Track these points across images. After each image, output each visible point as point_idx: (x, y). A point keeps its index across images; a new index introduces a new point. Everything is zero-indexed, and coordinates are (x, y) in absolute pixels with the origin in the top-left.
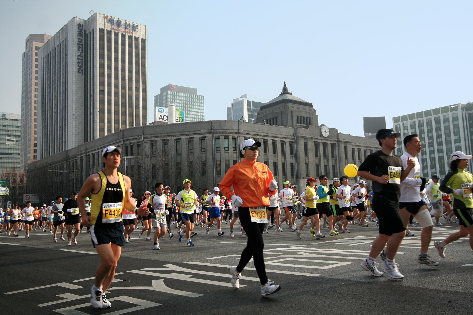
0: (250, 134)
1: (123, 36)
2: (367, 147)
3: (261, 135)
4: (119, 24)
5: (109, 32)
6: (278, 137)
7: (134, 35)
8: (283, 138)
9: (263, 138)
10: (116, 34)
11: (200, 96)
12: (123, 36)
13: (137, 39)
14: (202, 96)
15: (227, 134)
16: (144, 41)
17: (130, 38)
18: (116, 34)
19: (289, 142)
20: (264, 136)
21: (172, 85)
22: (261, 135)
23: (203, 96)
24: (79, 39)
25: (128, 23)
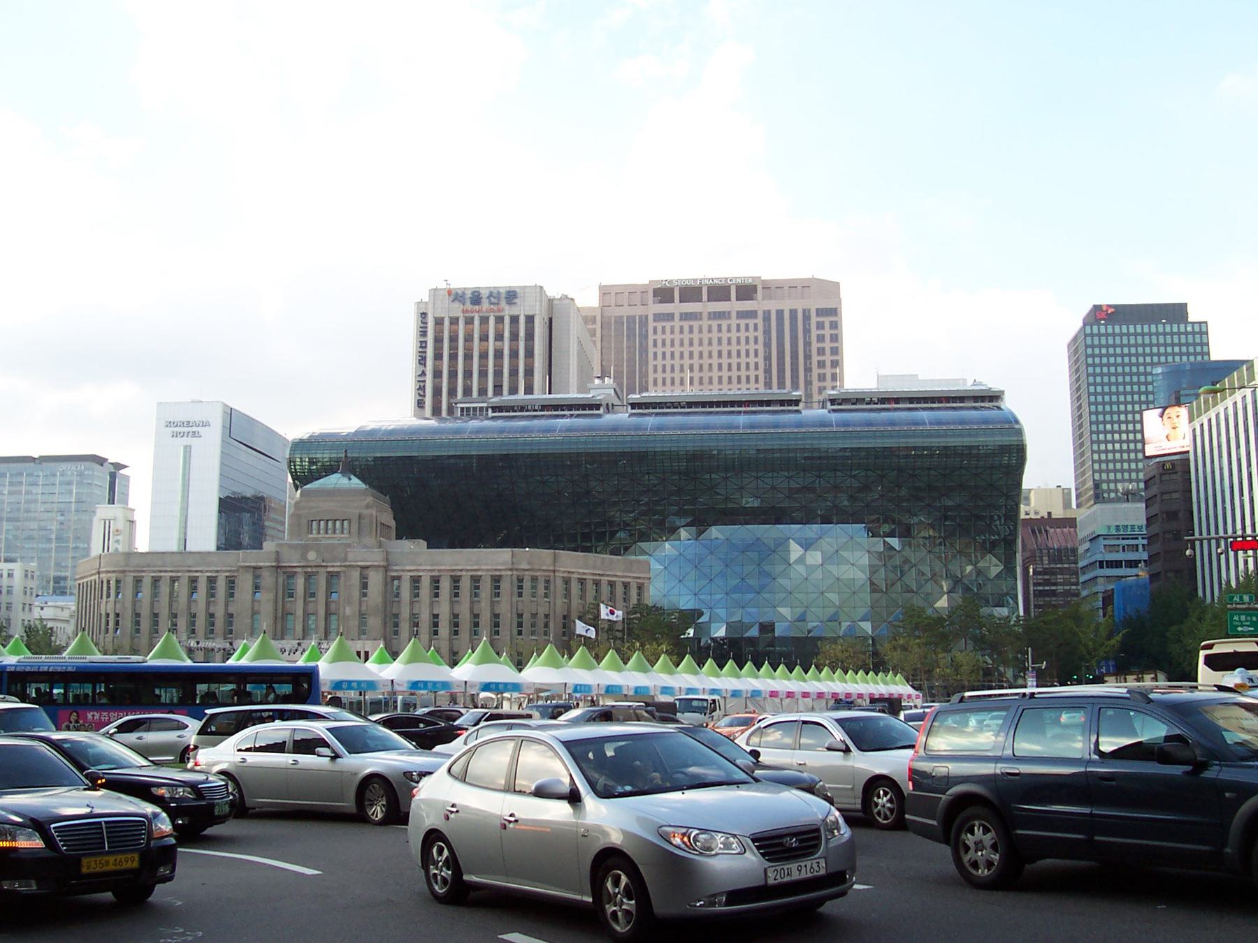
0: (143, 571)
1: (485, 320)
2: (439, 571)
3: (166, 571)
4: (476, 298)
5: (454, 321)
6: (201, 571)
7: (508, 312)
8: (211, 571)
9: (171, 574)
10: (469, 321)
11: (1193, 323)
12: (485, 320)
13: (514, 320)
14: (1200, 323)
15: (109, 575)
16: (530, 319)
17: (500, 320)
18: (469, 321)
19: (227, 577)
20: (171, 571)
21: (1101, 306)
22: (166, 571)
23: (1206, 323)
24: (421, 342)
25: (495, 291)
